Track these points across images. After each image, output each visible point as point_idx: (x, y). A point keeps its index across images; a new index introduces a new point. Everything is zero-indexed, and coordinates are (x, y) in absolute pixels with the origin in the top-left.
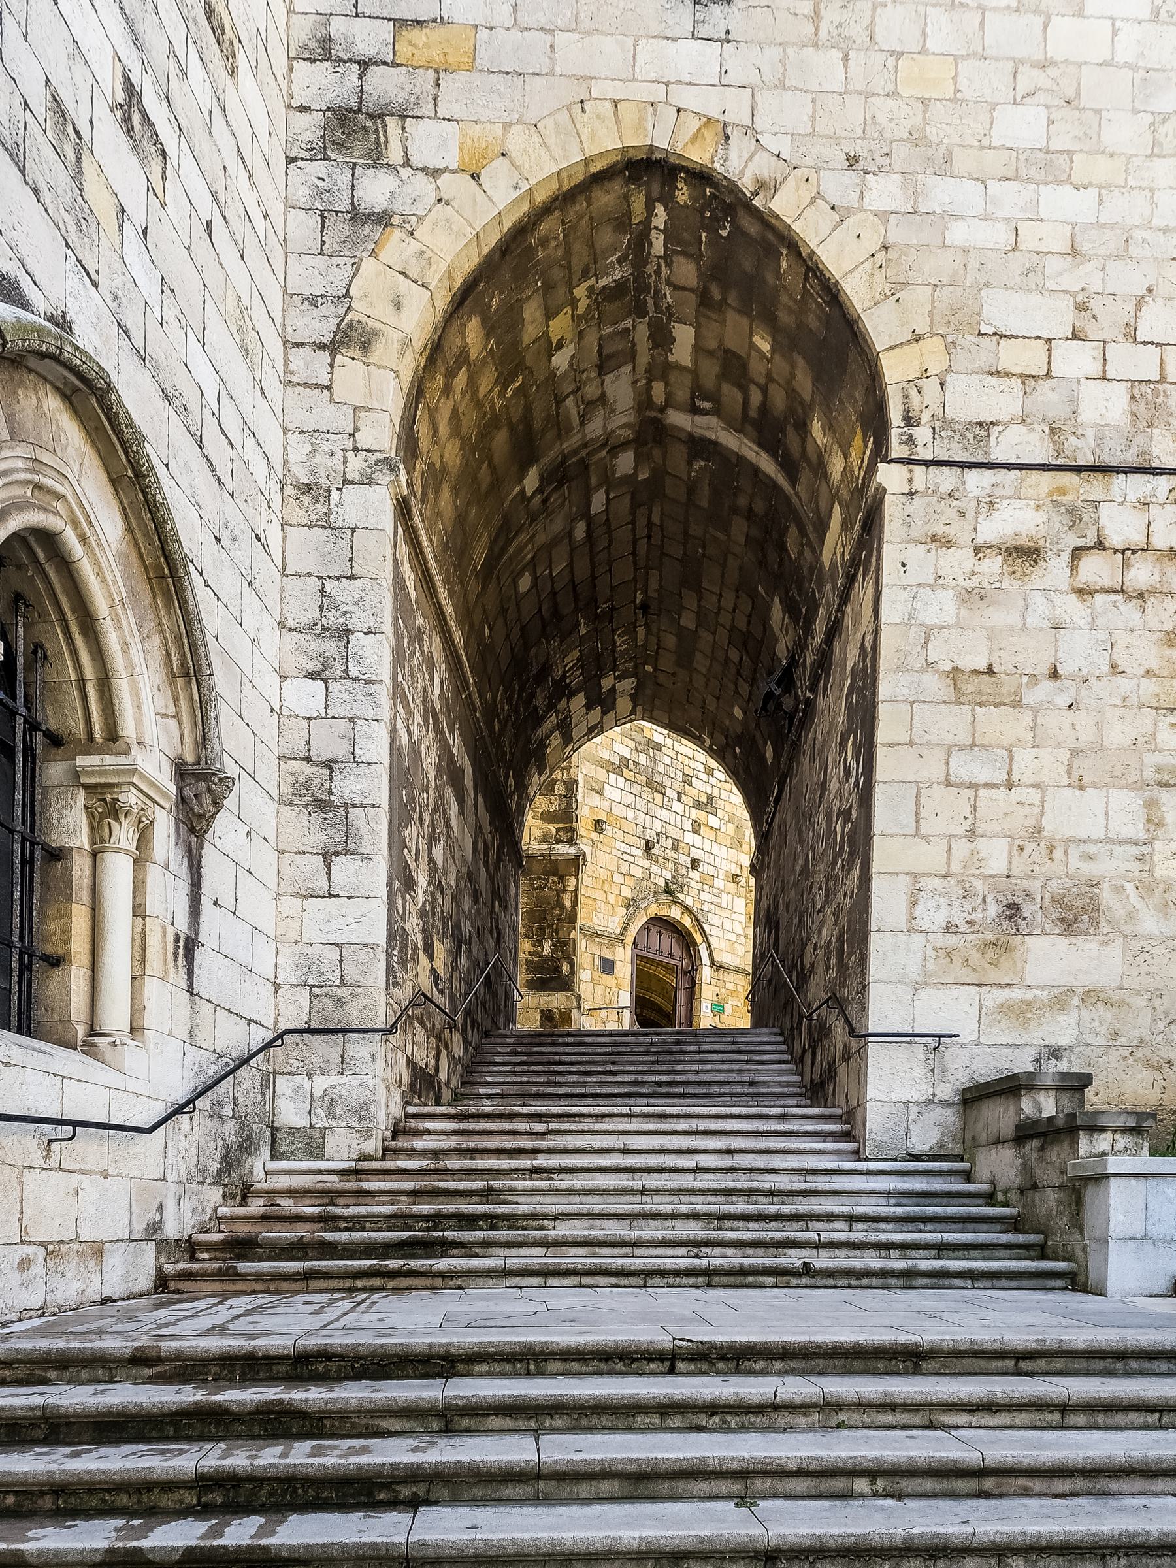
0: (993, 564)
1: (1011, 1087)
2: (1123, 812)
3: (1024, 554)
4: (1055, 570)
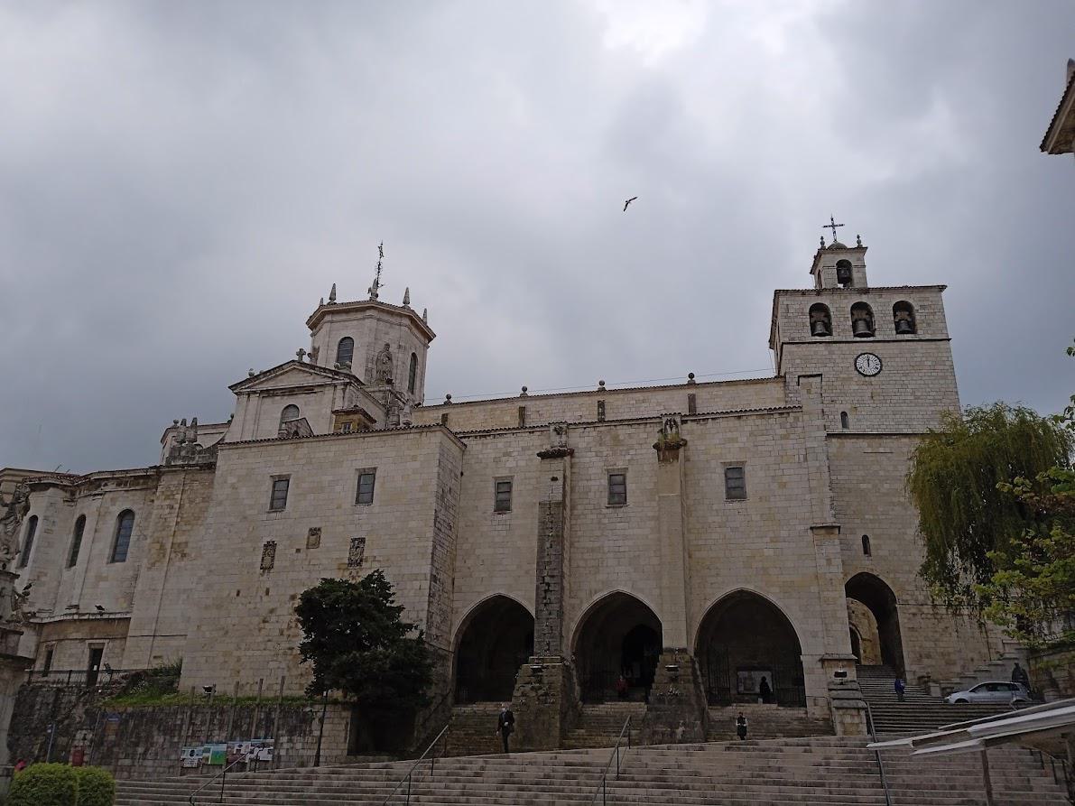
0: (911, 616)
1: (923, 677)
3: (914, 614)
4: (919, 616)
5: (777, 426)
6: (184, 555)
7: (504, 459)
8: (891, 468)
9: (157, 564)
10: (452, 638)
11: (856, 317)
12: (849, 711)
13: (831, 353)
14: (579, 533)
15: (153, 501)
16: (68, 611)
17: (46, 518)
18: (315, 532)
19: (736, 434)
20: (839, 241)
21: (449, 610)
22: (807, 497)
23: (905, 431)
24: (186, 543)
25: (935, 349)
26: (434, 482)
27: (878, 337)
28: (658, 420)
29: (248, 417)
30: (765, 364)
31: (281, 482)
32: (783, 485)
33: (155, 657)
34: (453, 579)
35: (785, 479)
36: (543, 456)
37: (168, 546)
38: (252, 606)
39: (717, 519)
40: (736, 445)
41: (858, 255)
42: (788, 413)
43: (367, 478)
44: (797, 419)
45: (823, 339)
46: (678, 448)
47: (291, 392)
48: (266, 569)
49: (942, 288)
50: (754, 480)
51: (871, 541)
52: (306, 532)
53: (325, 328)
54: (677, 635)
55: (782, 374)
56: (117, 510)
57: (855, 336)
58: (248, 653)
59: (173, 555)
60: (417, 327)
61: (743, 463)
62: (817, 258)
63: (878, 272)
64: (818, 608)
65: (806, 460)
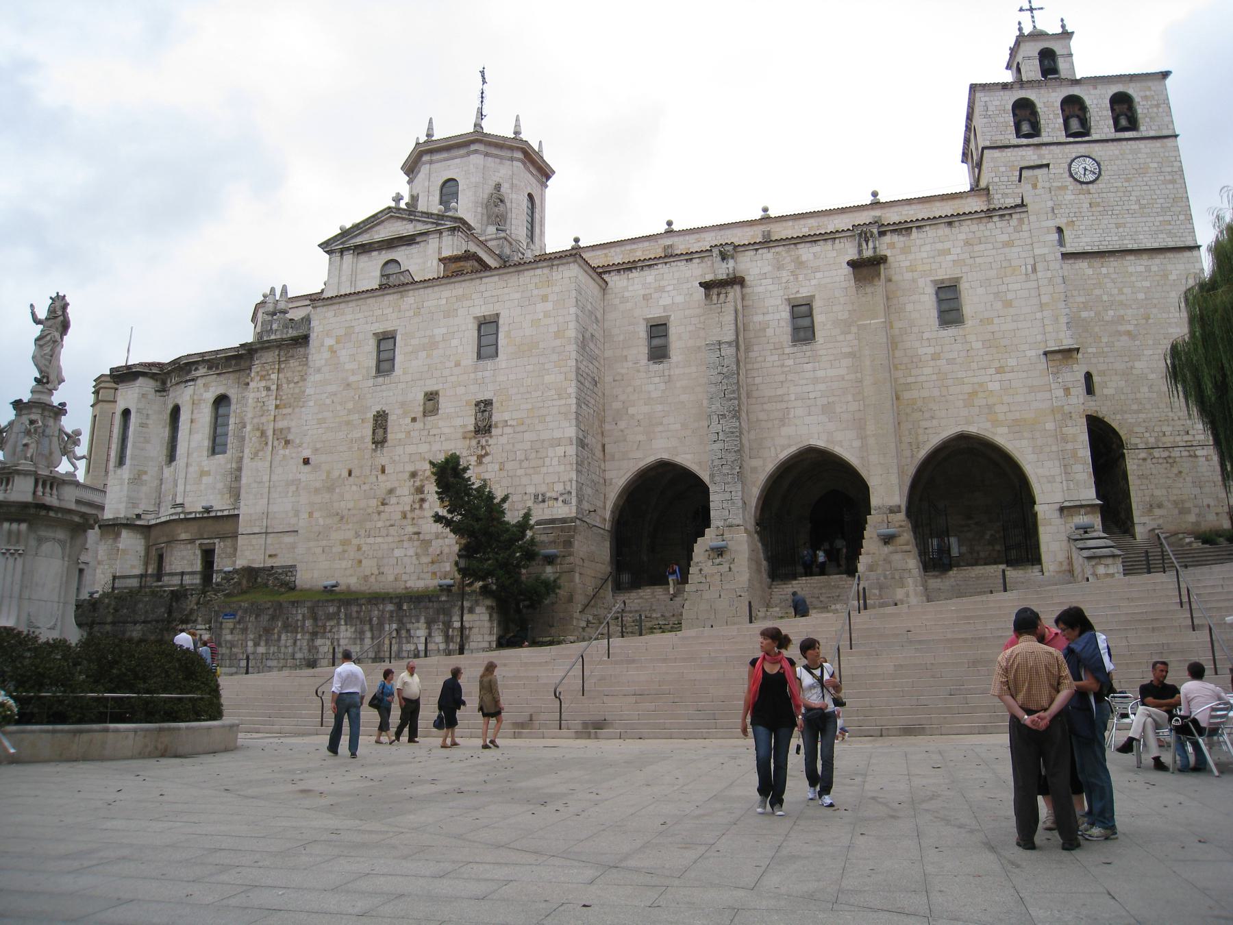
2: (1164, 492)
3: (1144, 459)
5: (999, 231)
6: (287, 442)
7: (655, 296)
8: (1115, 291)
9: (260, 454)
10: (608, 515)
11: (1067, 113)
12: (1103, 561)
14: (758, 380)
15: (248, 384)
16: (173, 511)
17: (139, 411)
18: (431, 397)
19: (947, 245)
20: (1039, 27)
21: (602, 481)
22: (1039, 315)
23: (1130, 247)
24: (289, 429)
26: (572, 325)
27: (1095, 137)
28: (849, 234)
29: (344, 278)
30: (959, 179)
31: (386, 340)
32: (1008, 304)
33: (270, 556)
34: (604, 446)
35: (1010, 296)
36: (707, 286)
37: (270, 433)
38: (366, 487)
39: (931, 350)
40: (949, 258)
41: (1064, 42)
43: (488, 327)
44: (1021, 221)
45: (1030, 141)
46: (879, 263)
47: (390, 244)
48: (379, 442)
49: (1165, 75)
50: (972, 301)
51: (1096, 379)
52: (421, 397)
53: (424, 170)
54: (887, 490)
55: (983, 184)
56: (210, 396)
57: (1068, 136)
58: (371, 540)
59: (276, 443)
60: (533, 162)
61: (958, 280)
62: (1013, 52)
63: (1089, 59)
64: (1054, 448)
65: (1034, 270)
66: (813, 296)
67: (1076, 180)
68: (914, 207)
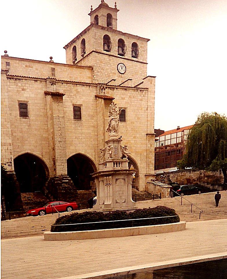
13: (110, 60)
25: (143, 66)
27: (126, 57)
40: (124, 100)
42: (143, 90)
44: (146, 93)
57: (118, 54)
61: (126, 108)
66: (82, 105)
67: (119, 71)
68: (66, 67)
